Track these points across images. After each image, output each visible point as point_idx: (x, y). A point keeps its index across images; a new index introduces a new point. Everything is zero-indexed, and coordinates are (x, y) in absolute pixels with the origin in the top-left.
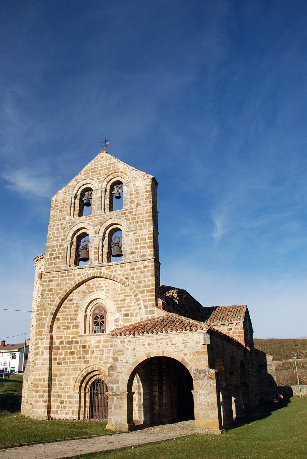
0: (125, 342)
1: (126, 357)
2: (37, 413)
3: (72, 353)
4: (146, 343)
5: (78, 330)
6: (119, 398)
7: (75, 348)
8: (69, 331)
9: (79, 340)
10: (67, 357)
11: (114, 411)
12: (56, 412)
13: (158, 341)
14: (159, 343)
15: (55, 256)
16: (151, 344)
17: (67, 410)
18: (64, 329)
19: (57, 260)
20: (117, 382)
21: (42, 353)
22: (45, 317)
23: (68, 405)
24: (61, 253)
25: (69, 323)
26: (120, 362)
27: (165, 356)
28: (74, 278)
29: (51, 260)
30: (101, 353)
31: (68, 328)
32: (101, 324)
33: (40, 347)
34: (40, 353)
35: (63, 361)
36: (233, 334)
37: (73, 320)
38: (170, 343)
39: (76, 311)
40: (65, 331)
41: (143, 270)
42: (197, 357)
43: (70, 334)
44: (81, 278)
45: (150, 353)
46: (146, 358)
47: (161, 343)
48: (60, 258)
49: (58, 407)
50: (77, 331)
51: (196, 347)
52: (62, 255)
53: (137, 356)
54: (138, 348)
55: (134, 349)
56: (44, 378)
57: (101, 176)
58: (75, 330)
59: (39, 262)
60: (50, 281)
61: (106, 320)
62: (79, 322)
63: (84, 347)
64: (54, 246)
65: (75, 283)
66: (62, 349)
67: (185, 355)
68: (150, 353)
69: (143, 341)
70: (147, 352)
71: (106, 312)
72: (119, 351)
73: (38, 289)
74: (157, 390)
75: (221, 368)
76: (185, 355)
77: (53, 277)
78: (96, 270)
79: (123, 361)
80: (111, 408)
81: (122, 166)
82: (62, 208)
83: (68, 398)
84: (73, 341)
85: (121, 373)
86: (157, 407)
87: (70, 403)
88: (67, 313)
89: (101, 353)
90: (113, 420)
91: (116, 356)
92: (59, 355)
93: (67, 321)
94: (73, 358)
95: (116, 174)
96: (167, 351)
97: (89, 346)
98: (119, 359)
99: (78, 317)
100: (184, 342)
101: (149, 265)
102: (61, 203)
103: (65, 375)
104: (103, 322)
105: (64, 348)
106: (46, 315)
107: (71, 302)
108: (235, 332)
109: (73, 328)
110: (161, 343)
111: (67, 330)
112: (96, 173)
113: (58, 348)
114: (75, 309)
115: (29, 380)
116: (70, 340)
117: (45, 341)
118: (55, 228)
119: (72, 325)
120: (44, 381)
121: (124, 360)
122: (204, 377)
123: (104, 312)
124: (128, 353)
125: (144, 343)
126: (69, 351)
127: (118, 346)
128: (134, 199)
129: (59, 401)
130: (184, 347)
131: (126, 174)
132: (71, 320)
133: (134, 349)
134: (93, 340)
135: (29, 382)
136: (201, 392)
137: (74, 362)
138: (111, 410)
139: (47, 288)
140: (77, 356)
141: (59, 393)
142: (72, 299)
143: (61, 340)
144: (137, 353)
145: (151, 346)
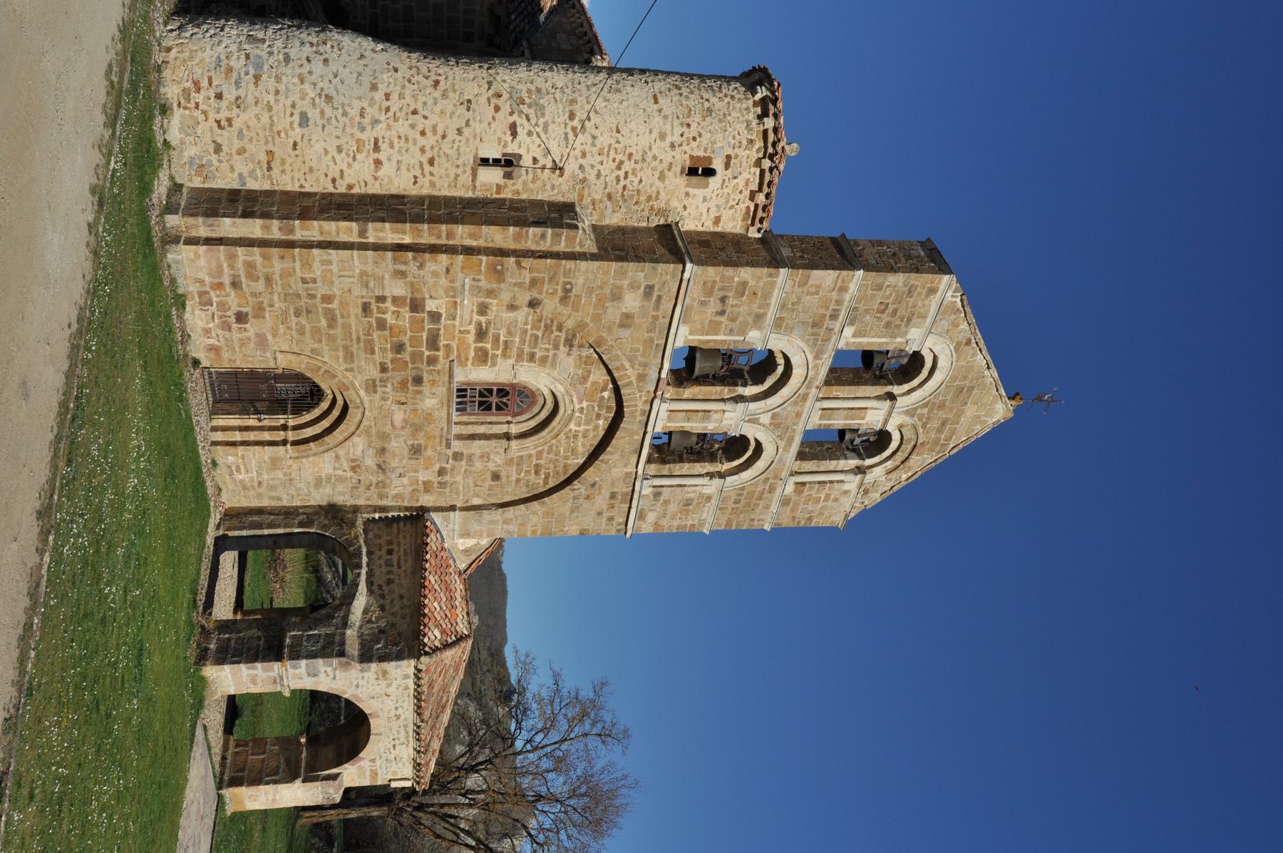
2: (192, 255)
3: (399, 348)
4: (400, 711)
5: (469, 363)
7: (416, 357)
8: (471, 338)
9: (439, 367)
10: (387, 332)
11: (244, 675)
12: (204, 299)
15: (730, 302)
17: (220, 332)
18: (479, 324)
21: (402, 274)
22: (527, 280)
23: (236, 335)
25: (497, 338)
28: (633, 367)
29: (723, 289)
31: (481, 334)
32: (481, 404)
33: (421, 267)
34: (402, 267)
35: (373, 321)
40: (472, 328)
41: (605, 515)
43: (462, 343)
44: (630, 384)
48: (718, 318)
49: (223, 306)
50: (467, 359)
54: (389, 703)
57: (931, 410)
58: (472, 353)
59: (754, 154)
60: (649, 290)
62: (494, 364)
63: (418, 380)
64: (767, 296)
65: (617, 369)
66: (412, 321)
70: (380, 713)
71: (514, 415)
72: (385, 673)
73: (650, 155)
76: (373, 761)
77: (659, 297)
78: (639, 418)
81: (921, 462)
82: (895, 311)
83: (257, 335)
87: (243, 343)
88: (529, 332)
90: (223, 674)
92: (393, 308)
93: (503, 332)
94: (383, 350)
95: (910, 447)
97: (419, 392)
98: (366, 674)
99: (512, 361)
103: (330, 326)
104: (489, 408)
105: (417, 325)
106: (534, 282)
109: (477, 349)
111: (473, 332)
113: (416, 306)
114: (539, 354)
115: (305, 131)
116: (442, 342)
117: (443, 281)
118: (834, 294)
119: (489, 346)
120: (304, 281)
121: (361, 682)
126: (405, 339)
129: (244, 310)
131: (889, 472)
132: (506, 342)
134: (433, 400)
135: (298, 130)
137: (373, 352)
139: (626, 283)
140: (388, 361)
141: (268, 309)
142: (571, 346)
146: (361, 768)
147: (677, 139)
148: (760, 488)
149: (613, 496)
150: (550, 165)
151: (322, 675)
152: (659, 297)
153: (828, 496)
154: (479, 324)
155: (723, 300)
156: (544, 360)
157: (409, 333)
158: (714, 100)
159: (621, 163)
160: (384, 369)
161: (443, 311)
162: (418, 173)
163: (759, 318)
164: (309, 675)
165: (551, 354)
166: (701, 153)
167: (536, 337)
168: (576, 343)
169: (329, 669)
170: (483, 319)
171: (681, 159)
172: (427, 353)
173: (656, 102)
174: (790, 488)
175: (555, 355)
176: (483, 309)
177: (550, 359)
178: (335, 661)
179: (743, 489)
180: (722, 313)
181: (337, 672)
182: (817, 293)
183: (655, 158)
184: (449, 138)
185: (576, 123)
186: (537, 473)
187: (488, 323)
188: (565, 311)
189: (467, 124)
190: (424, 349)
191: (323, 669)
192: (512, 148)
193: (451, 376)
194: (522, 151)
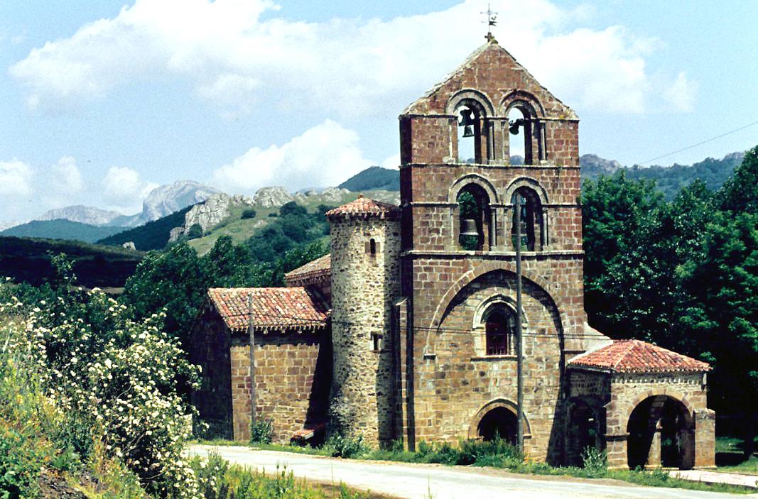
3: (465, 383)
19: (435, 235)
24: (441, 224)
27: (667, 394)
30: (509, 383)
46: (647, 396)
52: (443, 227)
56: (430, 421)
60: (426, 269)
67: (686, 394)
84: (464, 366)
89: (509, 383)
113: (443, 375)
122: (705, 417)
146: (692, 400)
147: (358, 261)
150: (374, 319)
151: (617, 418)
158: (340, 243)
159: (371, 285)
162: (382, 377)
166: (364, 248)
171: (367, 257)
173: (342, 271)
183: (368, 270)
184: (365, 364)
185: (355, 308)
189: (359, 356)
191: (613, 418)
192: (369, 335)
194: (370, 332)
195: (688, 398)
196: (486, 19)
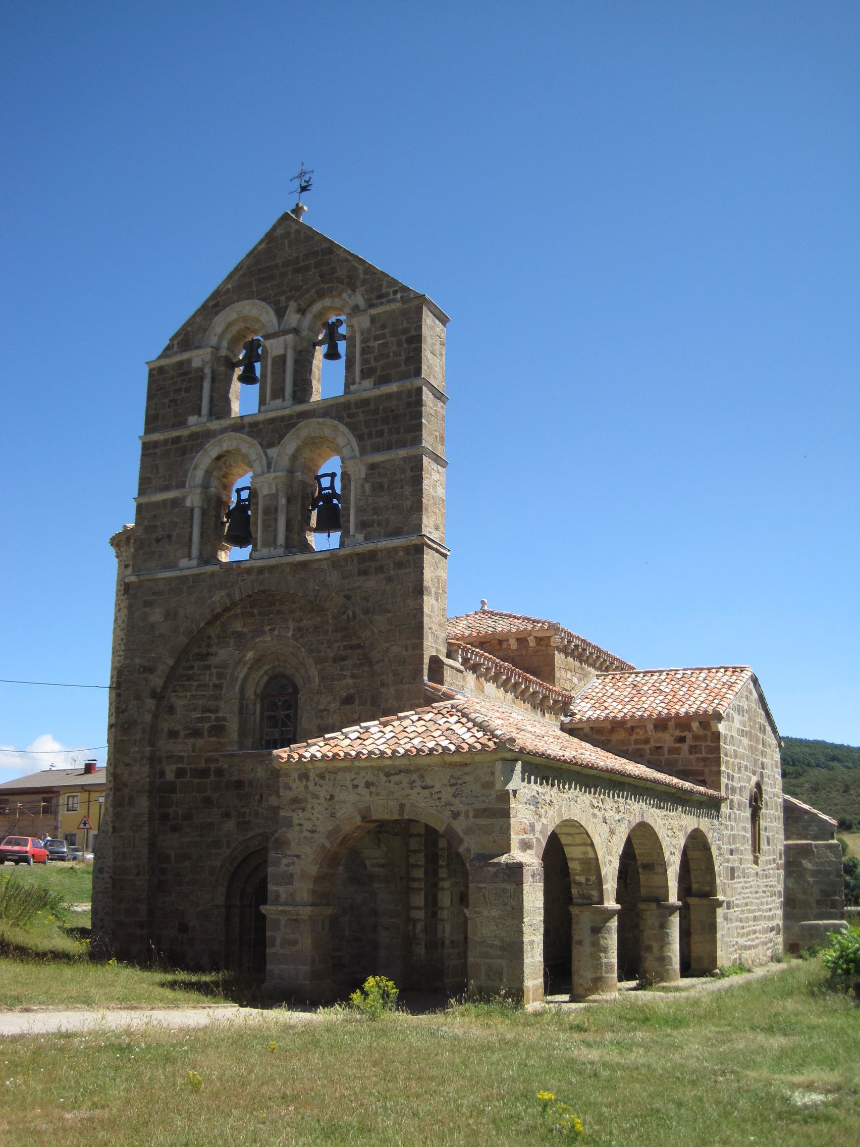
0: (311, 778)
1: (310, 816)
4: (362, 785)
6: (293, 920)
8: (200, 742)
9: (226, 766)
11: (281, 951)
13: (391, 778)
14: (392, 784)
16: (373, 784)
18: (186, 736)
20: (289, 879)
21: (131, 799)
22: (136, 702)
25: (200, 720)
26: (297, 828)
31: (196, 733)
34: (126, 799)
36: (691, 753)
37: (211, 711)
38: (418, 783)
39: (218, 687)
40: (190, 741)
41: (392, 573)
42: (482, 822)
45: (368, 809)
47: (396, 783)
51: (482, 795)
53: (338, 815)
54: (341, 796)
55: (332, 797)
58: (213, 739)
61: (296, 713)
62: (224, 719)
63: (239, 784)
65: (212, 610)
67: (456, 815)
68: (368, 809)
69: (353, 776)
71: (296, 691)
72: (295, 800)
74: (422, 904)
75: (587, 853)
76: (456, 815)
79: (305, 827)
80: (273, 945)
85: (298, 856)
86: (420, 950)
88: (194, 693)
91: (288, 814)
93: (195, 715)
96: (412, 805)
98: (296, 821)
99: (222, 705)
100: (453, 781)
101: (408, 561)
102: (173, 377)
106: (138, 697)
107: (203, 663)
108: (695, 747)
109: (210, 735)
110: (396, 783)
111: (192, 740)
112: (269, 285)
113: (171, 788)
116: (203, 765)
119: (207, 725)
120: (138, 874)
121: (308, 826)
123: (290, 690)
124: (316, 806)
125: (355, 782)
127: (294, 786)
128: (373, 363)
130: (454, 796)
132: (203, 712)
133: (332, 797)
136: (486, 913)
138: (274, 950)
142: (208, 654)
143: (180, 766)
144: (338, 807)
145: (373, 789)
146: (468, 831)
148: (361, 417)
149: (364, 573)
151: (291, 869)
152: (154, 594)
153: (376, 338)
154: (186, 736)
155: (158, 540)
156: (220, 676)
157: (195, 794)
160: (227, 815)
161: (175, 767)
163: (176, 503)
164: (291, 883)
165: (214, 671)
167: (199, 686)
168: (204, 651)
169: (285, 861)
170: (182, 734)
172: (212, 778)
174: (367, 383)
175: (216, 667)
176: (173, 734)
177: (219, 670)
178: (272, 855)
179: (360, 438)
180: (169, 537)
181: (289, 852)
182: (157, 466)
186: (344, 659)
187: (187, 728)
188: (161, 668)
190: (209, 780)
191: (283, 868)
193: (232, 756)
195: (459, 826)
196: (296, 185)
